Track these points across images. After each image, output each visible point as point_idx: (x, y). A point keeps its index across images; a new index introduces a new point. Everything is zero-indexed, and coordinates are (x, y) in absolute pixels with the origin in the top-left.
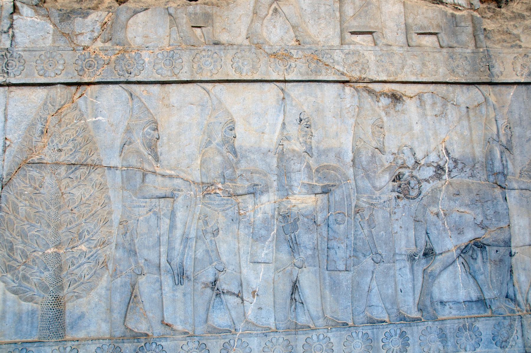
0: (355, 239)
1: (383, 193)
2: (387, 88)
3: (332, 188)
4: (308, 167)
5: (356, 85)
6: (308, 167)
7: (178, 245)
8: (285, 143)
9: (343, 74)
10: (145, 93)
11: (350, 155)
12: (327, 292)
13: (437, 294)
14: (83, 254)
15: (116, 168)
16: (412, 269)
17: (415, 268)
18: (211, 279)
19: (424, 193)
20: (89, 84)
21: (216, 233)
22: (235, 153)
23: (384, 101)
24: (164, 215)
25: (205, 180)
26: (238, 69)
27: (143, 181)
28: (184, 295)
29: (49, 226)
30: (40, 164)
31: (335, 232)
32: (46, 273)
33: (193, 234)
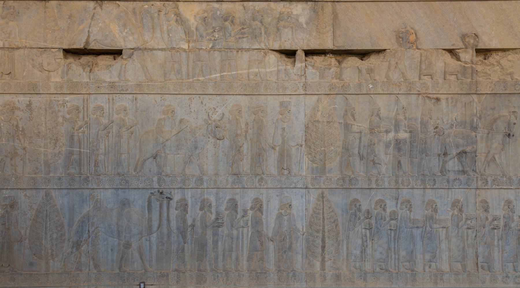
0: (419, 148)
1: (431, 133)
2: (435, 96)
3: (413, 131)
4: (405, 124)
5: (423, 95)
6: (405, 124)
7: (362, 148)
8: (397, 116)
9: (419, 91)
10: (351, 98)
11: (420, 120)
12: (409, 165)
13: (447, 168)
14: (332, 150)
15: (342, 123)
16: (439, 159)
17: (440, 159)
18: (372, 159)
19: (445, 134)
20: (332, 94)
21: (374, 144)
22: (380, 119)
23: (433, 101)
24: (357, 138)
25: (371, 127)
26: (383, 90)
27: (351, 127)
28: (364, 164)
29: (322, 141)
30: (318, 121)
31: (413, 146)
32: (322, 156)
33: (366, 144)
